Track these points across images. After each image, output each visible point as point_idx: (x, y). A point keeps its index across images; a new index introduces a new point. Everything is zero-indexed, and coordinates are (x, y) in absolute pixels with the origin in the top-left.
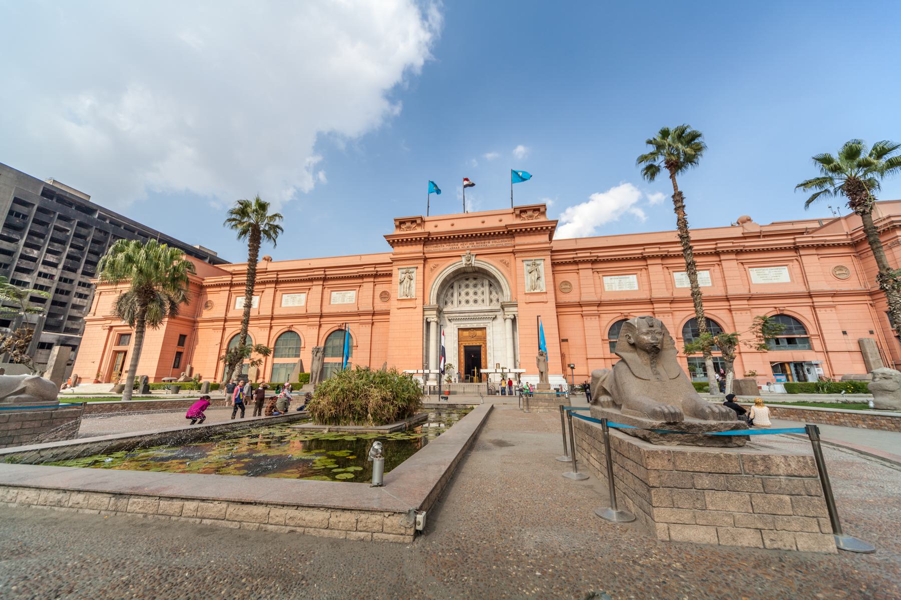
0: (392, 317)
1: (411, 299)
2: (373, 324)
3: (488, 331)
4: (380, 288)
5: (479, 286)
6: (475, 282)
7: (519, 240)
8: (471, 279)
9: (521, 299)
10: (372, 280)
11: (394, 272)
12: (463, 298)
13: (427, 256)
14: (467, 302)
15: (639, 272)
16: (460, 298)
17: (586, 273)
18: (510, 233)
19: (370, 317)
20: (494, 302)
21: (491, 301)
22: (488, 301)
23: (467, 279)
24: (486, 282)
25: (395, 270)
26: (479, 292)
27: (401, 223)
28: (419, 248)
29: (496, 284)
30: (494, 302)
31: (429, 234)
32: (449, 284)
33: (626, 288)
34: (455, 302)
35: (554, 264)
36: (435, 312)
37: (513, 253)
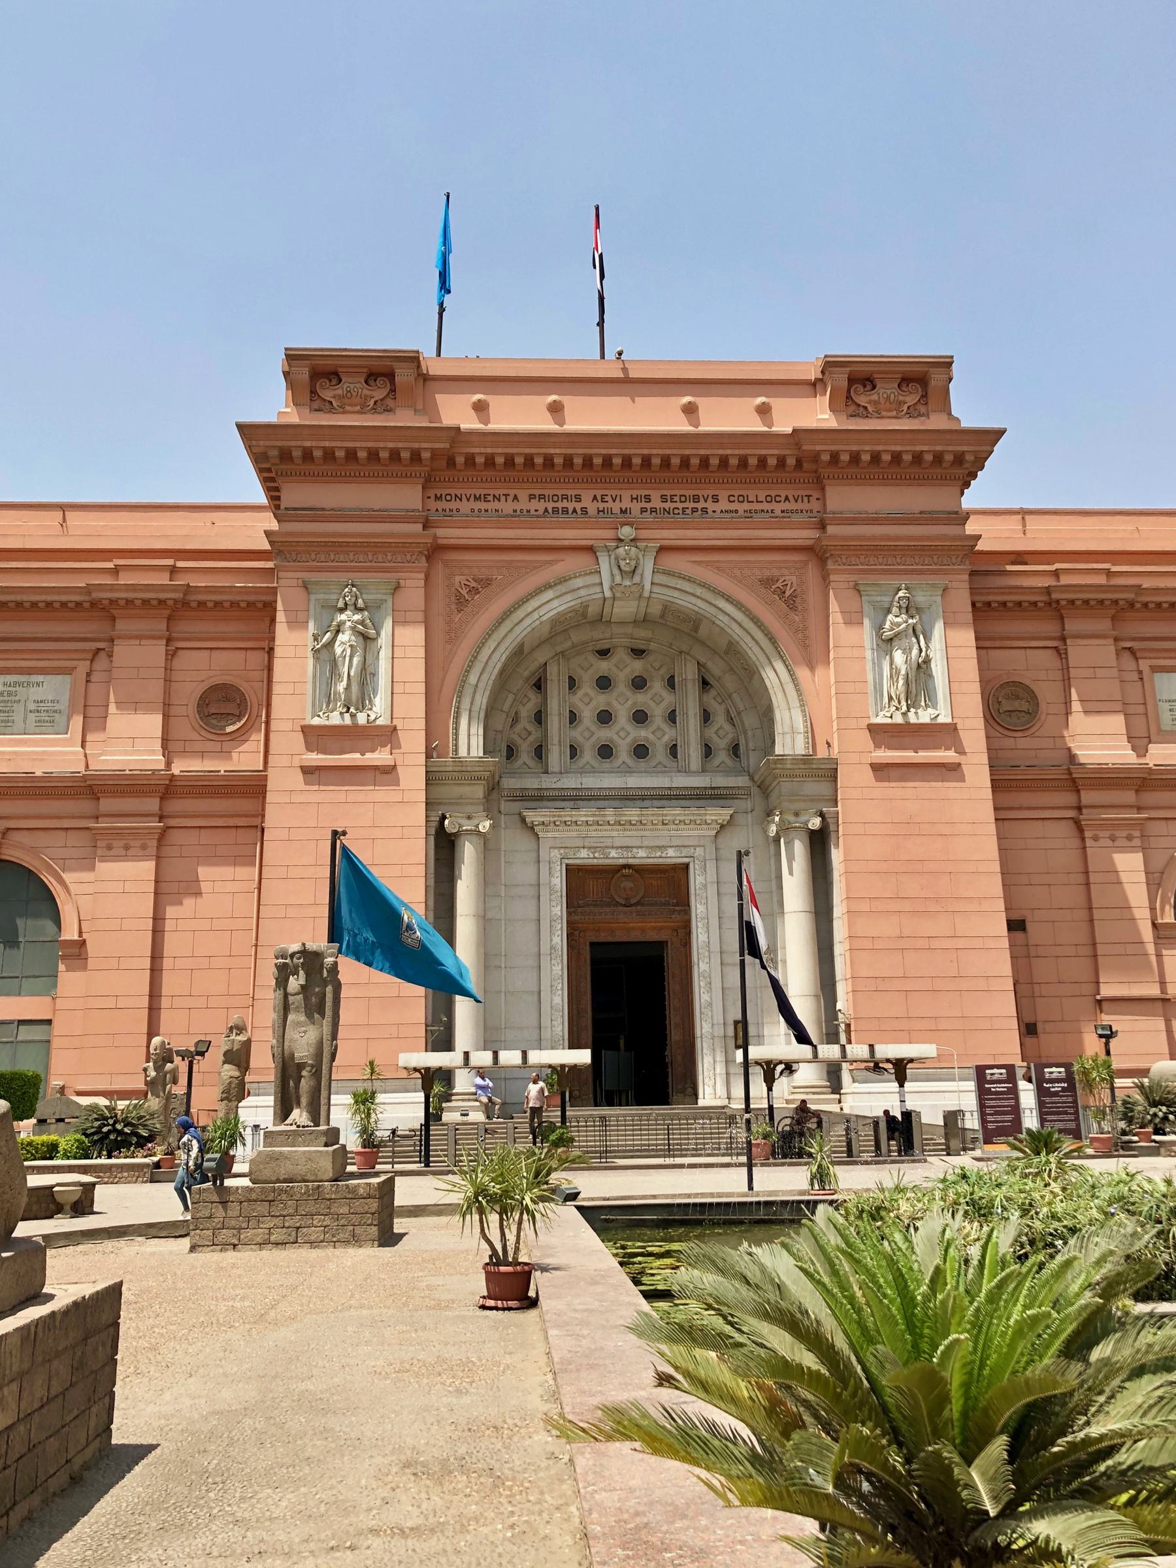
4: (202, 668)
5: (657, 686)
6: (637, 666)
7: (843, 498)
8: (621, 655)
12: (590, 734)
14: (606, 751)
16: (577, 734)
17: (1093, 654)
18: (802, 464)
19: (153, 804)
20: (722, 757)
21: (708, 751)
23: (604, 653)
26: (658, 713)
27: (314, 374)
34: (555, 756)
36: (479, 791)
37: (818, 554)
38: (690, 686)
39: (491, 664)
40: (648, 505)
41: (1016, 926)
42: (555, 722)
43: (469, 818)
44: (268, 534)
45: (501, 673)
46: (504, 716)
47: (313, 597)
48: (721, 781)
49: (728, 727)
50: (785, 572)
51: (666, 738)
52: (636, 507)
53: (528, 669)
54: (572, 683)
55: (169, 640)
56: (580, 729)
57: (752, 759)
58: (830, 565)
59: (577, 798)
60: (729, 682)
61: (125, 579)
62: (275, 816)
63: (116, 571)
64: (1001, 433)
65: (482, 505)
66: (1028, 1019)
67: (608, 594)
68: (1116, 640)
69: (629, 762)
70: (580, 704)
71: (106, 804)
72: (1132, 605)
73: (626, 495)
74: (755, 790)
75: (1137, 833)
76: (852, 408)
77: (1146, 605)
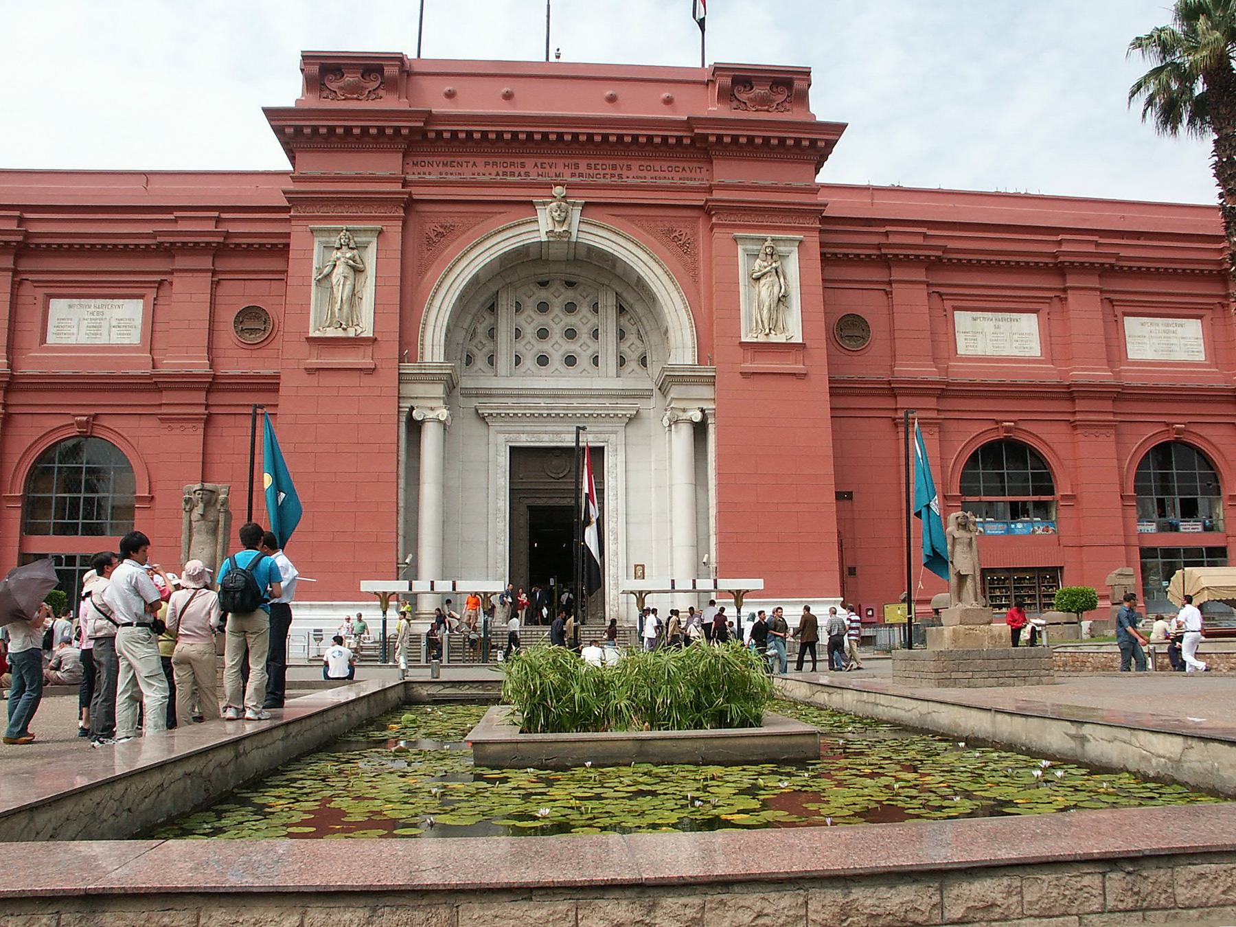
0: (286, 400)
1: (357, 342)
2: (208, 420)
3: (609, 460)
5: (585, 311)
6: (570, 295)
7: (726, 172)
8: (557, 286)
10: (207, 263)
11: (294, 243)
12: (531, 347)
13: (419, 193)
14: (543, 360)
15: (1045, 308)
16: (520, 347)
18: (696, 144)
19: (200, 397)
20: (633, 365)
21: (622, 361)
22: (612, 361)
23: (544, 284)
24: (608, 302)
25: (298, 233)
27: (323, 70)
28: (387, 164)
29: (639, 309)
30: (633, 365)
31: (429, 117)
33: (1009, 349)
35: (827, 260)
36: (439, 390)
38: (609, 310)
39: (452, 291)
40: (577, 172)
41: (843, 496)
43: (432, 409)
44: (285, 193)
45: (462, 297)
46: (464, 332)
47: (316, 240)
49: (638, 343)
50: (682, 224)
51: (590, 352)
52: (567, 172)
54: (519, 308)
55: (214, 273)
56: (523, 343)
58: (714, 220)
59: (519, 394)
60: (639, 309)
61: (181, 226)
63: (176, 220)
64: (844, 126)
65: (449, 169)
66: (849, 563)
67: (544, 238)
68: (928, 285)
69: (563, 368)
70: (524, 324)
71: (167, 397)
72: (939, 258)
73: (560, 162)
74: (656, 390)
75: (937, 429)
76: (735, 104)
77: (950, 260)
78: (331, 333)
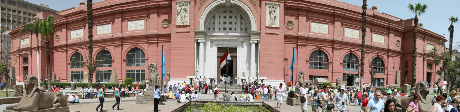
1: (186, 26)
5: (234, 18)
6: (230, 14)
8: (228, 12)
9: (264, 31)
12: (222, 26)
20: (244, 30)
21: (241, 29)
22: (239, 30)
23: (225, 12)
24: (239, 16)
26: (233, 23)
32: (212, 15)
34: (216, 29)
42: (216, 23)
48: (243, 34)
53: (212, 15)
54: (220, 17)
57: (248, 31)
60: (245, 18)
62: (172, 39)
78: (181, 24)
